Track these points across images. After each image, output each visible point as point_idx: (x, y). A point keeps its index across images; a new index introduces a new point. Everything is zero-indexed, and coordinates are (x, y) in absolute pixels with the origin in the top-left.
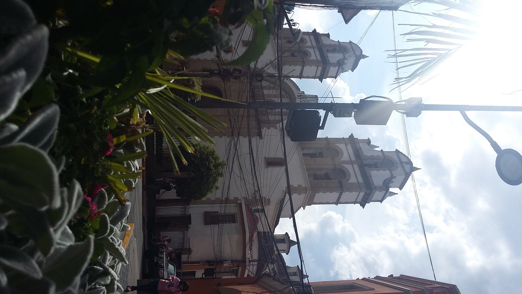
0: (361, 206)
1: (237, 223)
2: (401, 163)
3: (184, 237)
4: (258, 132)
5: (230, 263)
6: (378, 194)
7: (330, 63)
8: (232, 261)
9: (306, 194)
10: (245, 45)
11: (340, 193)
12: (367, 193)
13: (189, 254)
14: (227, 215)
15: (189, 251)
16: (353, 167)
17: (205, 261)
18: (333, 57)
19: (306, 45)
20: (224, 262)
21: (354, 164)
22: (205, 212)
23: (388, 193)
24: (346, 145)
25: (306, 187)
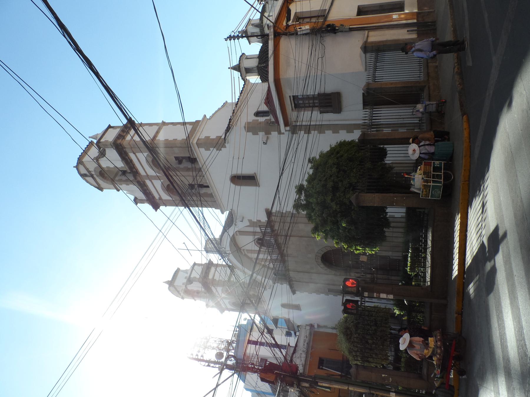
0: (133, 120)
1: (290, 96)
2: (92, 176)
3: (375, 69)
4: (272, 217)
5: (299, 30)
6: (111, 136)
7: (199, 282)
8: (296, 34)
9: (199, 137)
10: (298, 306)
11: (156, 139)
12: (122, 140)
13: (366, 42)
14: (307, 107)
15: (366, 48)
16: (146, 172)
17: (340, 31)
18: (196, 286)
19: (229, 300)
20: (309, 31)
21: (145, 176)
22: (340, 113)
23: (98, 139)
24: (160, 198)
25: (198, 148)
